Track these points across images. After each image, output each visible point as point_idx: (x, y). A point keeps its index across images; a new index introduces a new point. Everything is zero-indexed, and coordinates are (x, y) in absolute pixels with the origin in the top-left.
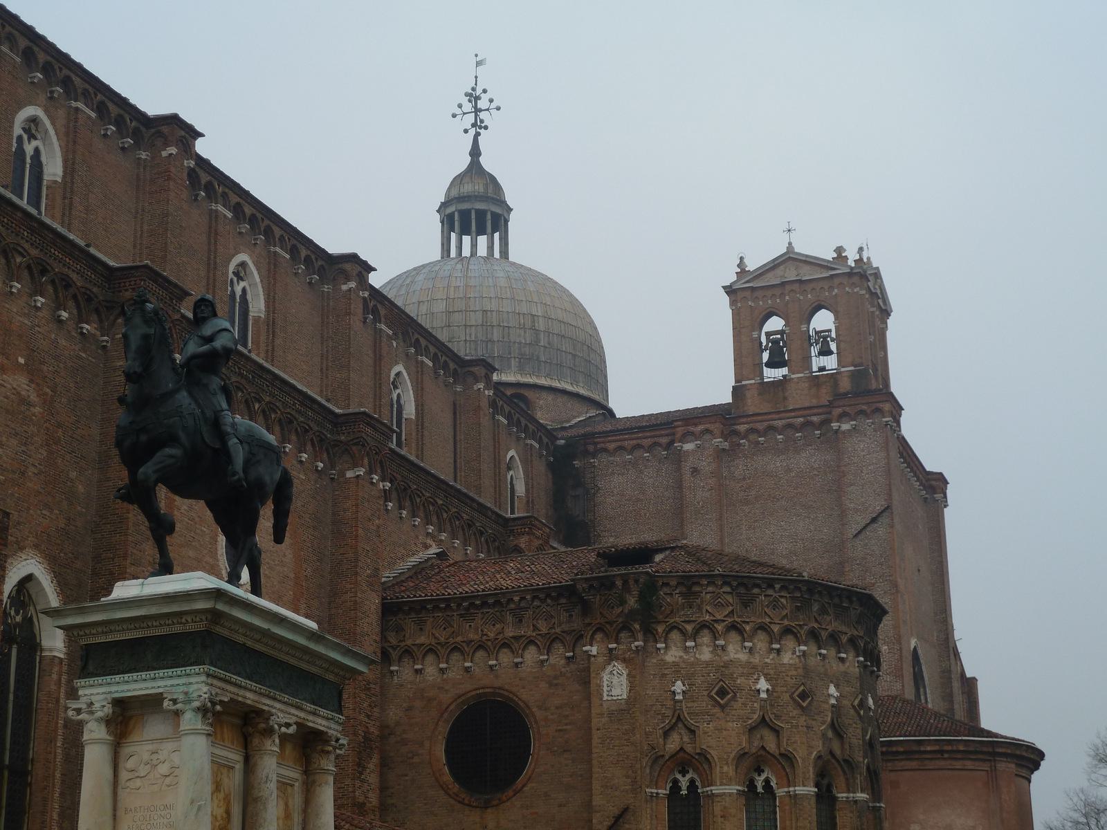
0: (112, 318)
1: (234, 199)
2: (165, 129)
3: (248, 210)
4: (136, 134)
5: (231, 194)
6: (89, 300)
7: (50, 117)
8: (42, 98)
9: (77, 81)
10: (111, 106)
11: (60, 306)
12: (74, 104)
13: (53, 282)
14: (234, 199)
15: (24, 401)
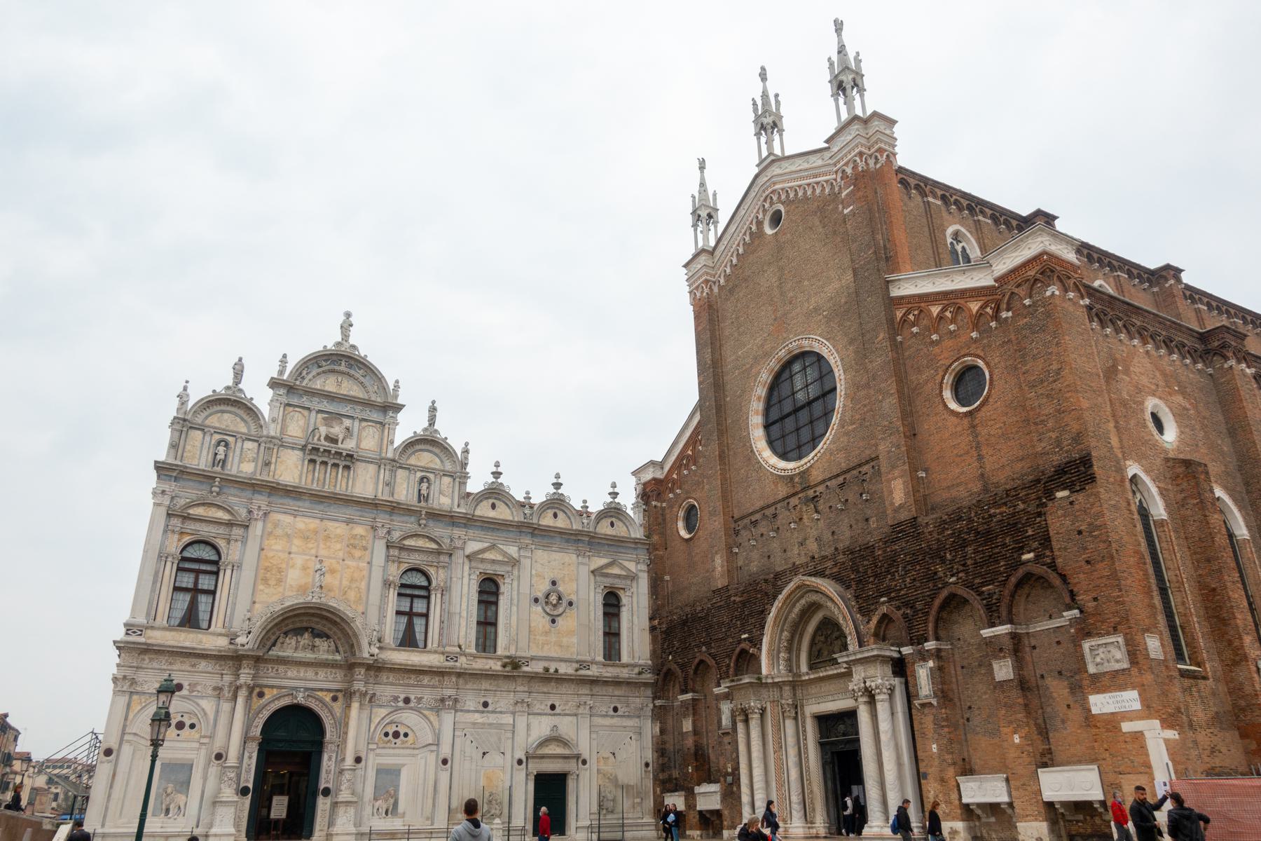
0: (1210, 358)
1: (1206, 300)
2: (1164, 273)
3: (1214, 304)
4: (1149, 280)
5: (1203, 298)
6: (1196, 351)
7: (1107, 283)
8: (1101, 275)
9: (1114, 262)
10: (1133, 270)
11: (1184, 358)
12: (1115, 274)
13: (1177, 346)
14: (1206, 300)
15: (1185, 409)
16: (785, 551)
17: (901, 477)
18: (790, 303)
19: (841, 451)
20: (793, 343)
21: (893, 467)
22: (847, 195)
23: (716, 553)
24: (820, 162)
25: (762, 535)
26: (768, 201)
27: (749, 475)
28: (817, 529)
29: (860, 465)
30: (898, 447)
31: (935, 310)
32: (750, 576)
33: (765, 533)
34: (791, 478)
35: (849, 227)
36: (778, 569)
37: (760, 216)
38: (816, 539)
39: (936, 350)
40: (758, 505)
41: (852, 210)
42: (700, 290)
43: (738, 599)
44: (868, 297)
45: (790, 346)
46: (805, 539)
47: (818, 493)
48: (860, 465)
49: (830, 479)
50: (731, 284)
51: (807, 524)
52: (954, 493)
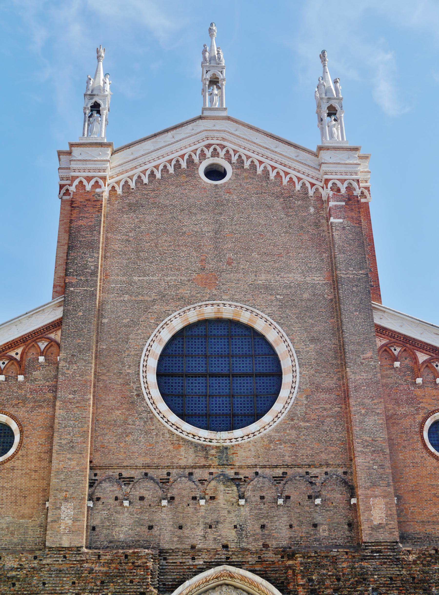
16: (181, 528)
17: (385, 497)
18: (229, 264)
19: (285, 443)
20: (228, 307)
21: (374, 485)
22: (333, 205)
23: (66, 499)
24: (293, 156)
25: (142, 498)
26: (211, 149)
27: (130, 421)
28: (237, 516)
29: (309, 466)
30: (382, 466)
31: (422, 357)
32: (111, 542)
33: (146, 496)
34: (205, 448)
35: (336, 237)
36: (166, 546)
37: (196, 159)
38: (235, 527)
39: (419, 392)
40: (140, 461)
41: (341, 223)
42: (92, 182)
43: (97, 568)
44: (356, 311)
45: (221, 305)
46: (218, 522)
47: (240, 476)
48: (309, 466)
49: (264, 467)
50: (132, 199)
51: (222, 505)
52: (429, 529)
